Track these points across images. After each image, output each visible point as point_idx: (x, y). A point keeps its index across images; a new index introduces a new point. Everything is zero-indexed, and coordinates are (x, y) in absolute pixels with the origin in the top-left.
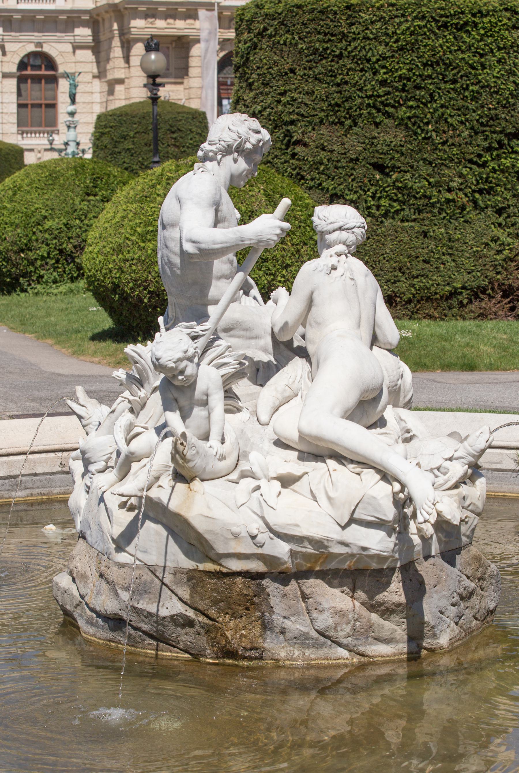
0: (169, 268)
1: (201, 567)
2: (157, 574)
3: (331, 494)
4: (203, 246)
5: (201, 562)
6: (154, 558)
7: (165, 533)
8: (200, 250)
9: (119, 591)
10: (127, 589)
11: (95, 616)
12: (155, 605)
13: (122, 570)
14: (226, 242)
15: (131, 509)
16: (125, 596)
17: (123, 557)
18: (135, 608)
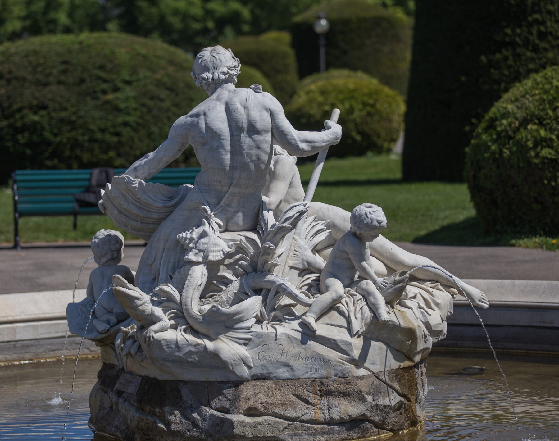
0: (255, 164)
1: (403, 365)
2: (381, 378)
3: (439, 301)
4: (317, 144)
5: (402, 362)
6: (377, 368)
7: (385, 347)
8: (313, 148)
9: (366, 396)
10: (369, 394)
11: (326, 426)
12: (388, 398)
13: (363, 381)
14: (328, 141)
15: (359, 336)
16: (369, 398)
17: (362, 372)
18: (377, 405)
